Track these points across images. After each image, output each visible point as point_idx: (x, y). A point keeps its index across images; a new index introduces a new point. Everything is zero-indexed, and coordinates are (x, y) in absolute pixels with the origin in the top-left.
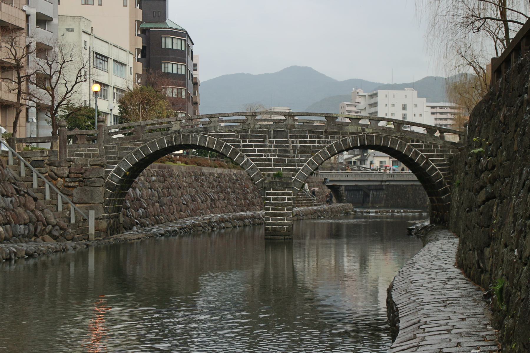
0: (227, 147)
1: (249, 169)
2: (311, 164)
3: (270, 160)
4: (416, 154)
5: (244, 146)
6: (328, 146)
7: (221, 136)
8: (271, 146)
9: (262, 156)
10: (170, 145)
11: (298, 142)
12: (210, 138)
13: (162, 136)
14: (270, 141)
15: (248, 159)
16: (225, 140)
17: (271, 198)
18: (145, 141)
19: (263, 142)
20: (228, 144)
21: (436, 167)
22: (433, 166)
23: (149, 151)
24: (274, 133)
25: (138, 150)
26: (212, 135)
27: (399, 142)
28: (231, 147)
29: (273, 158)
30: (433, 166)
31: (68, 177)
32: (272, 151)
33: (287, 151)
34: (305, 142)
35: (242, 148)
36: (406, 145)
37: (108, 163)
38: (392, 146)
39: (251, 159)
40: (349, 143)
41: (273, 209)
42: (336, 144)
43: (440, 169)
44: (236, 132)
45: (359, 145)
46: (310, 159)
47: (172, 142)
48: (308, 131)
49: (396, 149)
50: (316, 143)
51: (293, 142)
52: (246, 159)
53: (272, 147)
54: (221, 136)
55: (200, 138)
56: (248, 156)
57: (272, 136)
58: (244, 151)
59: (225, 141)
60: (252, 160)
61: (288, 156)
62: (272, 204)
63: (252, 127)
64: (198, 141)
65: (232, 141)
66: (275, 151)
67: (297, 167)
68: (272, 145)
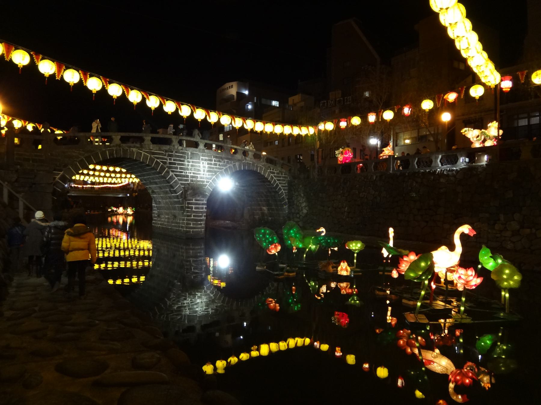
1: (173, 183)
3: (187, 176)
4: (272, 178)
5: (170, 163)
6: (224, 168)
8: (188, 165)
9: (182, 172)
10: (111, 157)
11: (206, 163)
12: (144, 154)
14: (188, 161)
15: (172, 175)
16: (156, 157)
17: (193, 207)
19: (183, 161)
20: (158, 160)
22: (280, 187)
25: (83, 160)
27: (264, 169)
28: (160, 163)
29: (190, 175)
30: (280, 187)
31: (16, 181)
33: (199, 170)
34: (211, 164)
35: (168, 165)
36: (267, 171)
37: (55, 170)
38: (260, 172)
39: (174, 174)
41: (194, 216)
43: (283, 189)
44: (164, 151)
47: (113, 154)
49: (262, 174)
50: (218, 164)
51: (203, 163)
52: (171, 173)
53: (189, 166)
55: (137, 153)
56: (173, 171)
57: (189, 157)
58: (169, 168)
59: (156, 157)
61: (199, 174)
62: (194, 212)
63: (176, 148)
64: (135, 155)
67: (205, 183)
68: (189, 164)
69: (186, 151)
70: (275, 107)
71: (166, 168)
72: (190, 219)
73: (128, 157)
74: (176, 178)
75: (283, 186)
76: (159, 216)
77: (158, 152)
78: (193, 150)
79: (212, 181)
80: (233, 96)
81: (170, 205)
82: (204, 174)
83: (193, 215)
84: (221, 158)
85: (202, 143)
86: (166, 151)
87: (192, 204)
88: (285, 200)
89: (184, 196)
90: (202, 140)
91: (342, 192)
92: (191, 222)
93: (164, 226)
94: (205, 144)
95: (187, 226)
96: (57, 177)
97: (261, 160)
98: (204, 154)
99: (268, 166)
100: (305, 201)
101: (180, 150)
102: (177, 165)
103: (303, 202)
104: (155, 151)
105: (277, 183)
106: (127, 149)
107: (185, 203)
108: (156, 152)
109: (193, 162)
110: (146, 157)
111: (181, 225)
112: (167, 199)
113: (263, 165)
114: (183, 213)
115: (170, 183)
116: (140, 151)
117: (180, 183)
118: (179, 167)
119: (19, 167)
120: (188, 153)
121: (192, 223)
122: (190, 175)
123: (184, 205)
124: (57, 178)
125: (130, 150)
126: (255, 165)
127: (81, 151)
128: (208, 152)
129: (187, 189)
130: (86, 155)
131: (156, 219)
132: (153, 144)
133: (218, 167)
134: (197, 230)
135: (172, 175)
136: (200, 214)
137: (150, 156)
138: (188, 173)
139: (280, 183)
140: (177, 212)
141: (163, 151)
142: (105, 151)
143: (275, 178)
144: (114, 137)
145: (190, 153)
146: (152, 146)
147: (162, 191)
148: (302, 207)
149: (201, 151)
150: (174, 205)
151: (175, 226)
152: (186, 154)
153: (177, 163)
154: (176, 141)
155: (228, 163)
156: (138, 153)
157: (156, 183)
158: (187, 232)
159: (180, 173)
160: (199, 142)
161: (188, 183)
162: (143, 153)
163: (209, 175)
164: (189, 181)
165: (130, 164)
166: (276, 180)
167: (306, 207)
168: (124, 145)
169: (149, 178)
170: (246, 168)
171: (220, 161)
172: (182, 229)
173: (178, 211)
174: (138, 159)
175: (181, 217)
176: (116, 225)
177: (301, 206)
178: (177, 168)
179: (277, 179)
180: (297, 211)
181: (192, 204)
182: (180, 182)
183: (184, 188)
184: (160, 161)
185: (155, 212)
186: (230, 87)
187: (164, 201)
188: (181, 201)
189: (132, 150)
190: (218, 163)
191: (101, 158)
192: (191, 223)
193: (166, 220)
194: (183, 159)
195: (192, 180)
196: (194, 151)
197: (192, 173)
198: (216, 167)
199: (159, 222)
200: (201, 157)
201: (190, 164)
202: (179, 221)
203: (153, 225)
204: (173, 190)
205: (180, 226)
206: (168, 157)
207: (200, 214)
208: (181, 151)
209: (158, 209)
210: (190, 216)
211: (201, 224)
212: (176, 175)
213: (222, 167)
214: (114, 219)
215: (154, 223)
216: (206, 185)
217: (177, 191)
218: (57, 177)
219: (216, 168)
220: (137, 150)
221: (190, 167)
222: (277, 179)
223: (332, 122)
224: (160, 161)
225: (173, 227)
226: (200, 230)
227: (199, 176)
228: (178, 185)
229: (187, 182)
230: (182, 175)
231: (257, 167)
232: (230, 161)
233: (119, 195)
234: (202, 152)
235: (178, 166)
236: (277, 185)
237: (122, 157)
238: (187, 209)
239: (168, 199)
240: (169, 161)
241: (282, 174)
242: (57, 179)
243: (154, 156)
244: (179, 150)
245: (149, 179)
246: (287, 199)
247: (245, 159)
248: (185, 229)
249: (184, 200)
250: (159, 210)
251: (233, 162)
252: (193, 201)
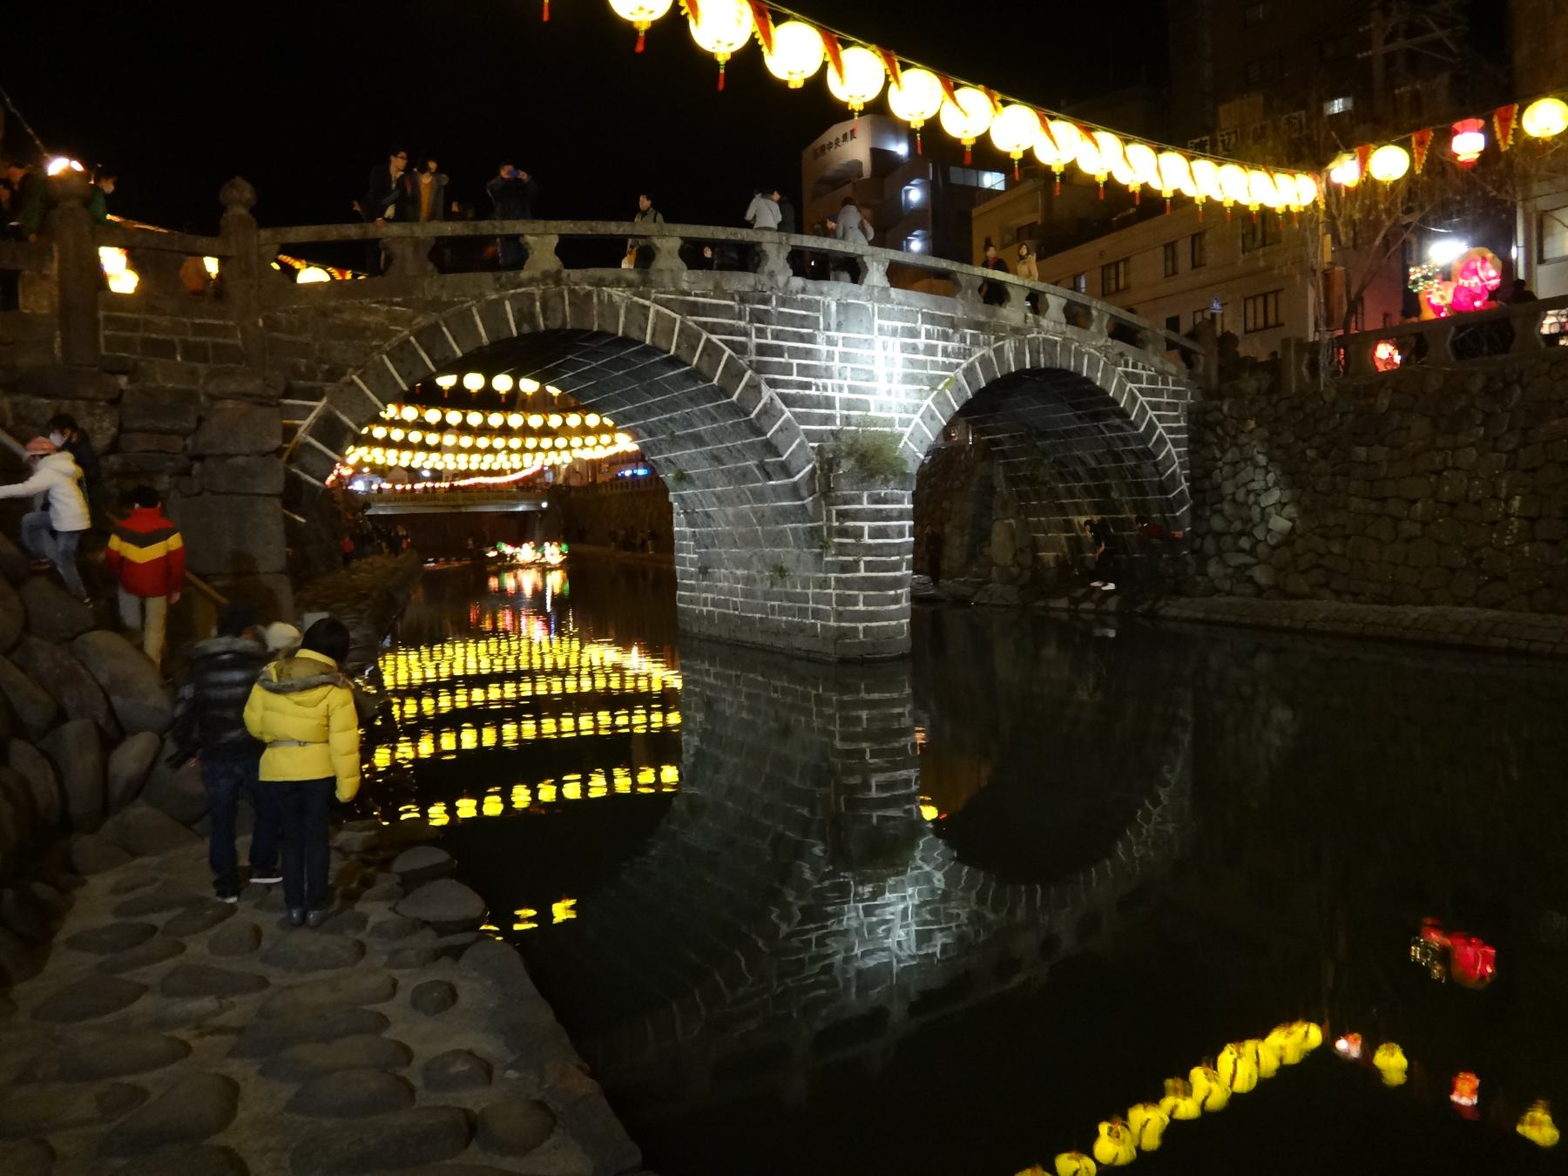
0: (712, 351)
1: (777, 431)
2: (928, 419)
3: (829, 403)
4: (1133, 398)
5: (762, 350)
6: (965, 364)
7: (694, 309)
8: (830, 356)
9: (807, 386)
10: (526, 329)
12: (657, 312)
13: (497, 290)
14: (828, 337)
15: (772, 399)
16: (706, 323)
17: (862, 528)
18: (436, 305)
20: (714, 338)
21: (1166, 436)
23: (451, 348)
24: (838, 311)
25: (408, 342)
26: (665, 304)
27: (1102, 363)
28: (723, 352)
32: (836, 373)
33: (870, 376)
34: (915, 349)
35: (754, 358)
36: (1114, 372)
38: (1091, 375)
39: (780, 395)
40: (1008, 360)
41: (870, 566)
42: (984, 361)
43: (1172, 441)
44: (737, 298)
45: (1028, 366)
47: (531, 317)
48: (923, 314)
49: (1098, 383)
51: (885, 348)
52: (767, 393)
53: (833, 359)
54: (694, 309)
55: (628, 311)
56: (773, 384)
57: (833, 322)
58: (760, 368)
59: (704, 325)
60: (784, 398)
62: (870, 550)
63: (781, 284)
64: (622, 320)
69: (818, 298)
70: (991, 193)
71: (745, 371)
72: (852, 578)
73: (595, 329)
74: (786, 409)
75: (1170, 431)
76: (704, 571)
77: (711, 304)
78: (845, 291)
79: (922, 417)
80: (860, 164)
81: (759, 528)
83: (865, 562)
84: (954, 324)
85: (879, 262)
86: (743, 301)
87: (856, 515)
88: (1181, 484)
89: (824, 483)
90: (878, 250)
91: (1482, 431)
92: (857, 593)
93: (732, 612)
94: (887, 264)
95: (841, 608)
96: (300, 426)
97: (1093, 328)
98: (889, 306)
99: (1117, 351)
100: (1276, 484)
101: (797, 293)
102: (786, 355)
103: (1267, 489)
104: (701, 299)
105: (1151, 418)
106: (589, 295)
107: (824, 513)
108: (704, 304)
110: (665, 326)
111: (811, 605)
112: (742, 503)
113: (1098, 349)
114: (820, 556)
115: (765, 434)
116: (641, 301)
117: (802, 433)
118: (798, 364)
119: (123, 381)
120: (828, 306)
121: (861, 598)
122: (837, 395)
123: (820, 523)
124: (301, 430)
125: (599, 296)
126: (1073, 347)
127: (398, 304)
128: (902, 298)
129: (831, 456)
130: (421, 321)
131: (693, 582)
132: (690, 268)
133: (940, 358)
134: (885, 623)
135: (772, 399)
136: (893, 558)
137: (682, 322)
138: (833, 390)
139: (1159, 417)
140: (788, 554)
141: (733, 299)
142: (499, 303)
143: (1141, 398)
144: (530, 239)
146: (687, 278)
147: (722, 471)
148: (1263, 509)
149: (876, 294)
150: (778, 523)
151: (783, 611)
152: (819, 311)
153: (789, 347)
154: (779, 252)
156: (631, 307)
157: (698, 440)
158: (843, 634)
159: (801, 392)
160: (865, 259)
161: (832, 432)
162: (654, 308)
164: (835, 425)
165: (594, 364)
166: (1148, 408)
167: (1284, 505)
168: (576, 274)
169: (670, 419)
170: (1042, 361)
171: (946, 337)
172: (819, 623)
173: (796, 551)
174: (635, 334)
175: (810, 574)
176: (513, 601)
177: (1257, 503)
178: (787, 369)
179: (1148, 402)
180: (1238, 525)
181: (856, 515)
182: (802, 427)
183: (820, 451)
184: (720, 340)
185: (687, 557)
186: (845, 136)
187: (730, 510)
188: (810, 508)
189: (610, 296)
190: (941, 344)
191: (483, 334)
192: (857, 596)
193: (739, 586)
194: (811, 331)
195: (847, 417)
196: (847, 295)
197: (846, 390)
198: (932, 361)
199: (704, 595)
200: (877, 322)
202: (799, 590)
203: (681, 605)
204: (774, 464)
205: (807, 609)
206: (751, 321)
207: (893, 558)
208: (800, 296)
209: (698, 544)
210: (853, 567)
211: (896, 600)
212: (784, 398)
213: (954, 361)
214: (510, 582)
215: (682, 598)
216: (901, 435)
217: (793, 466)
218: (300, 426)
219: (935, 365)
220: (628, 293)
221: (836, 364)
222: (1148, 402)
223: (1404, 144)
224: (720, 340)
225: (773, 613)
226: (894, 623)
228: (797, 441)
229: (829, 428)
230: (809, 396)
231: (1079, 356)
232: (981, 336)
233: (517, 505)
234: (879, 301)
235: (791, 361)
236: (1151, 427)
237: (569, 327)
238: (836, 540)
239: (749, 502)
240: (755, 340)
241: (1165, 383)
242: (302, 435)
243: (695, 322)
244: (791, 292)
245: (670, 425)
246: (1186, 481)
247: (1038, 325)
248: (832, 623)
249: (823, 502)
250: (707, 548)
251: (993, 337)
252: (861, 504)
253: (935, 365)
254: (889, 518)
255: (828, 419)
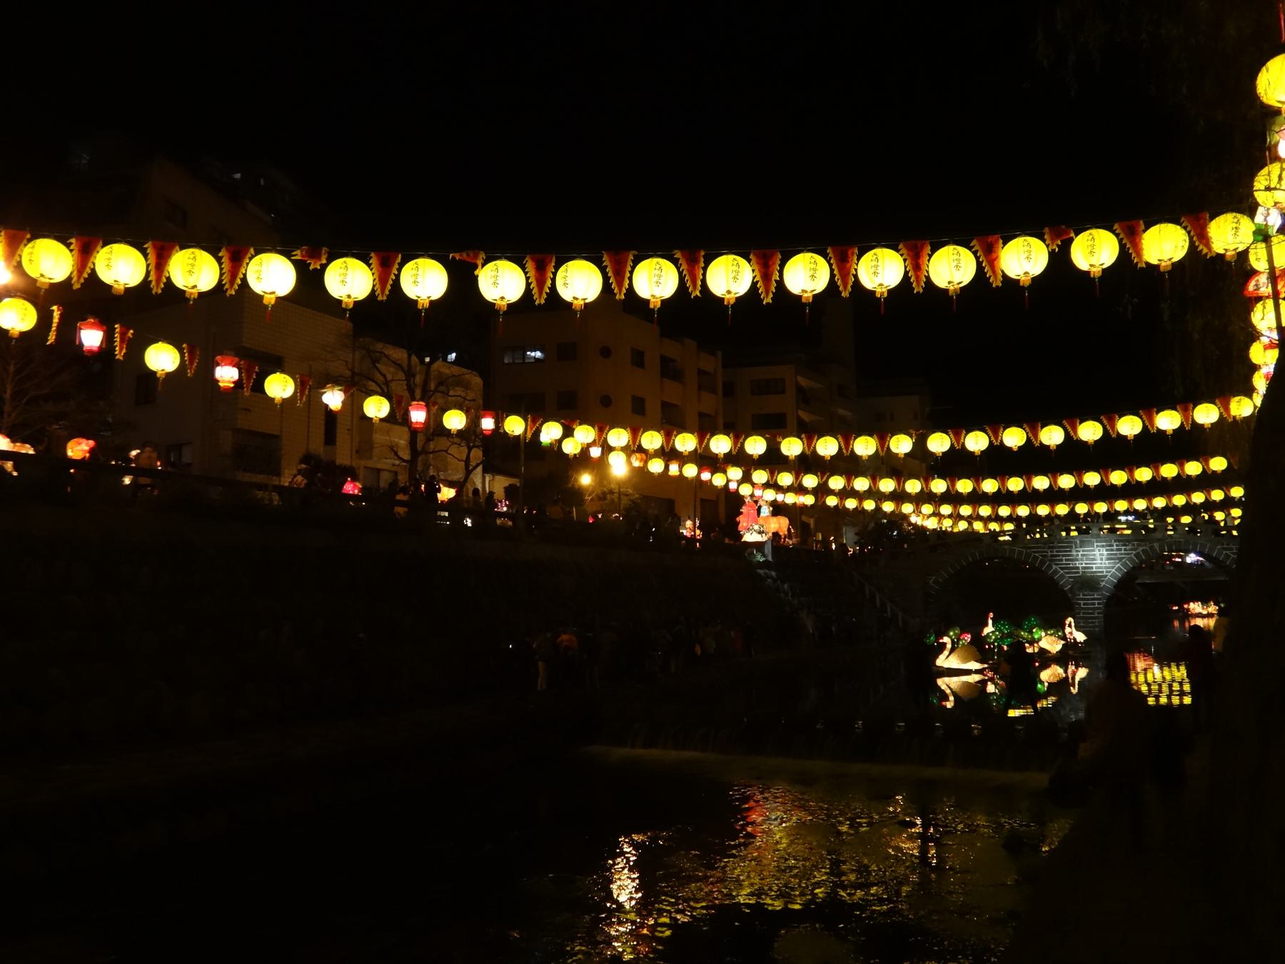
3: (1078, 568)
5: (1052, 556)
8: (1078, 555)
9: (1069, 564)
19: (1070, 551)
29: (1080, 566)
33: (1094, 559)
34: (1112, 550)
41: (1083, 613)
42: (1143, 551)
46: (1117, 565)
52: (1054, 567)
57: (1078, 545)
58: (1051, 561)
59: (1033, 552)
60: (1061, 568)
62: (1083, 609)
65: (1039, 552)
66: (1082, 560)
67: (1105, 574)
82: (1101, 564)
109: (1083, 551)
122: (1080, 566)
133: (1123, 552)
145: (1078, 542)
155: (1138, 545)
162: (1017, 549)
163: (1109, 563)
178: (1062, 560)
190: (1123, 548)
200: (1095, 544)
201: (1080, 553)
212: (1060, 568)
216: (1107, 576)
227: (1094, 566)
253: (1122, 554)
254: (1088, 599)
255: (1078, 573)
